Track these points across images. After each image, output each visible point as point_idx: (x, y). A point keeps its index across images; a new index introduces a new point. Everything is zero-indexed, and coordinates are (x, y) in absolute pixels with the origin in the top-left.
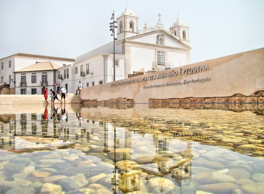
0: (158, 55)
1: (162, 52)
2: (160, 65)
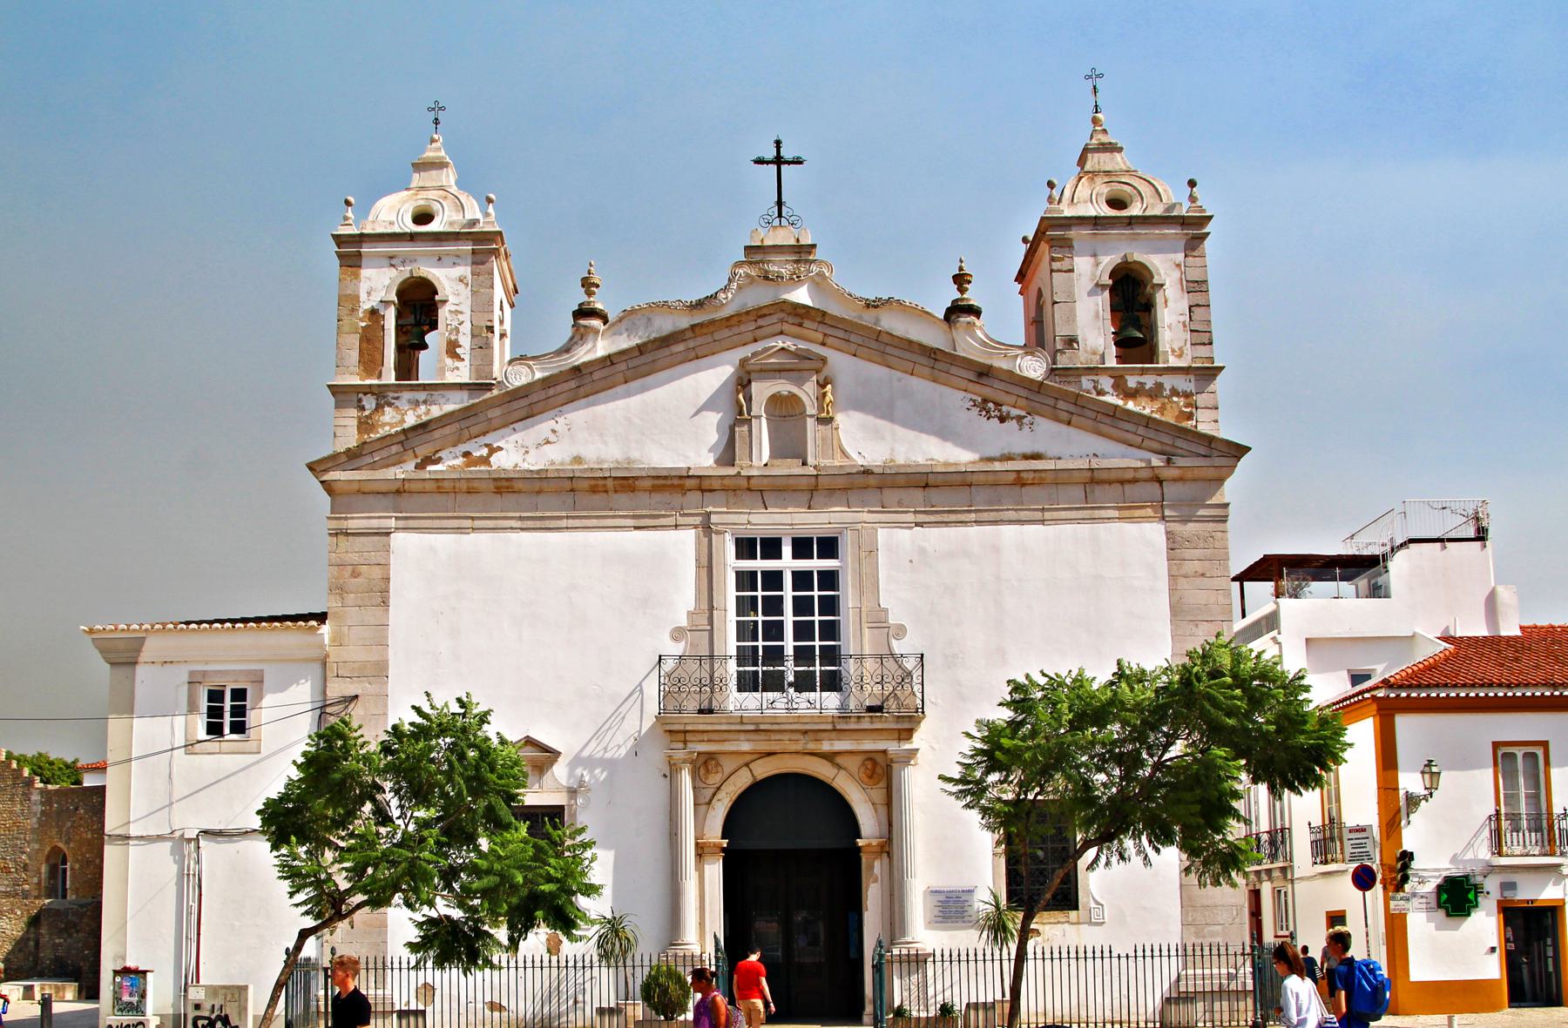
0: (746, 580)
1: (802, 548)
2: (774, 683)
